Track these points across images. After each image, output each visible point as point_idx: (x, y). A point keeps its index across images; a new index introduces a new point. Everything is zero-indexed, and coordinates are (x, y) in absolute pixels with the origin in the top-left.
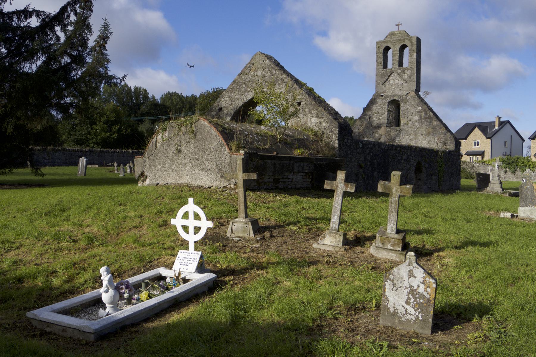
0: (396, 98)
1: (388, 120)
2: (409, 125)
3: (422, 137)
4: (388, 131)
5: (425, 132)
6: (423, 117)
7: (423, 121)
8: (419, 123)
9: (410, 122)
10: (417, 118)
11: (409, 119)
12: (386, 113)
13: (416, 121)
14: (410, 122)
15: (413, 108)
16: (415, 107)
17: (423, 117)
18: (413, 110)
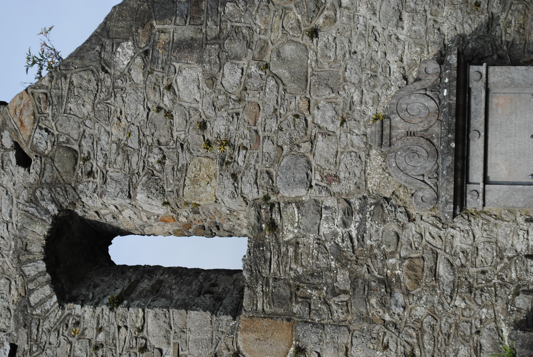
0: (40, 231)
1: (186, 306)
2: (241, 134)
3: (324, 37)
4: (274, 298)
5: (295, 15)
6: (186, 32)
7: (212, 30)
8: (225, 58)
9: (219, 127)
10: (188, 78)
11: (195, 138)
12: (133, 315)
13: (212, 80)
14: (219, 127)
15: (117, 103)
16: (113, 91)
17: (186, 32)
18: (132, 106)
